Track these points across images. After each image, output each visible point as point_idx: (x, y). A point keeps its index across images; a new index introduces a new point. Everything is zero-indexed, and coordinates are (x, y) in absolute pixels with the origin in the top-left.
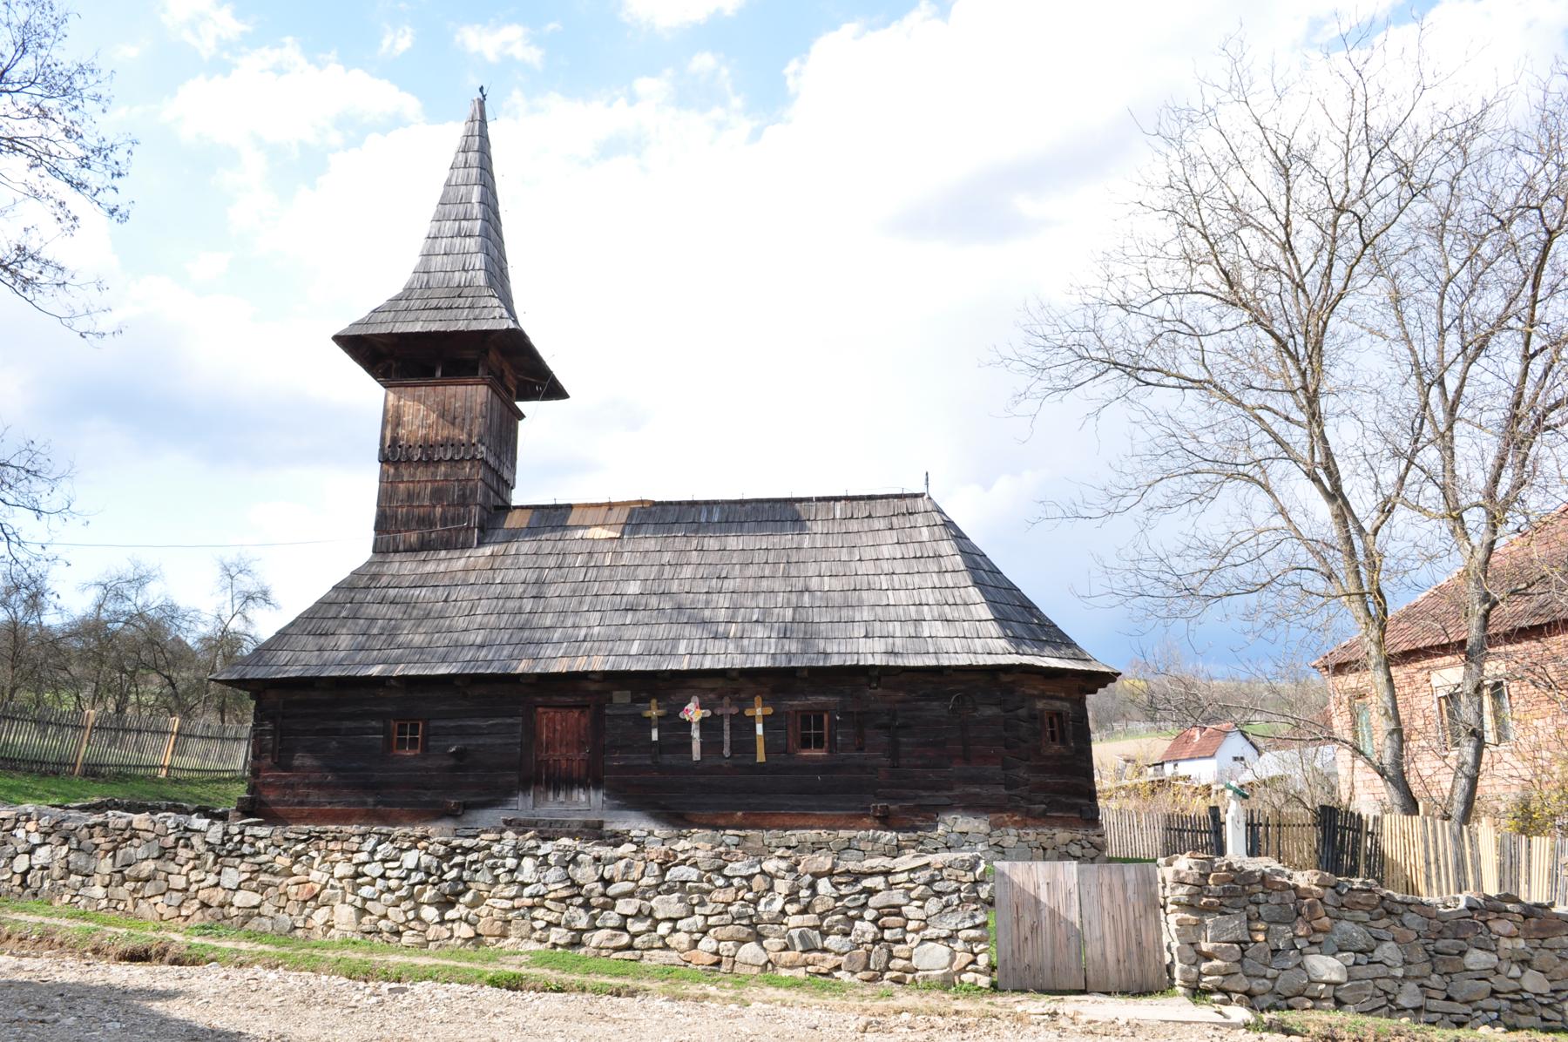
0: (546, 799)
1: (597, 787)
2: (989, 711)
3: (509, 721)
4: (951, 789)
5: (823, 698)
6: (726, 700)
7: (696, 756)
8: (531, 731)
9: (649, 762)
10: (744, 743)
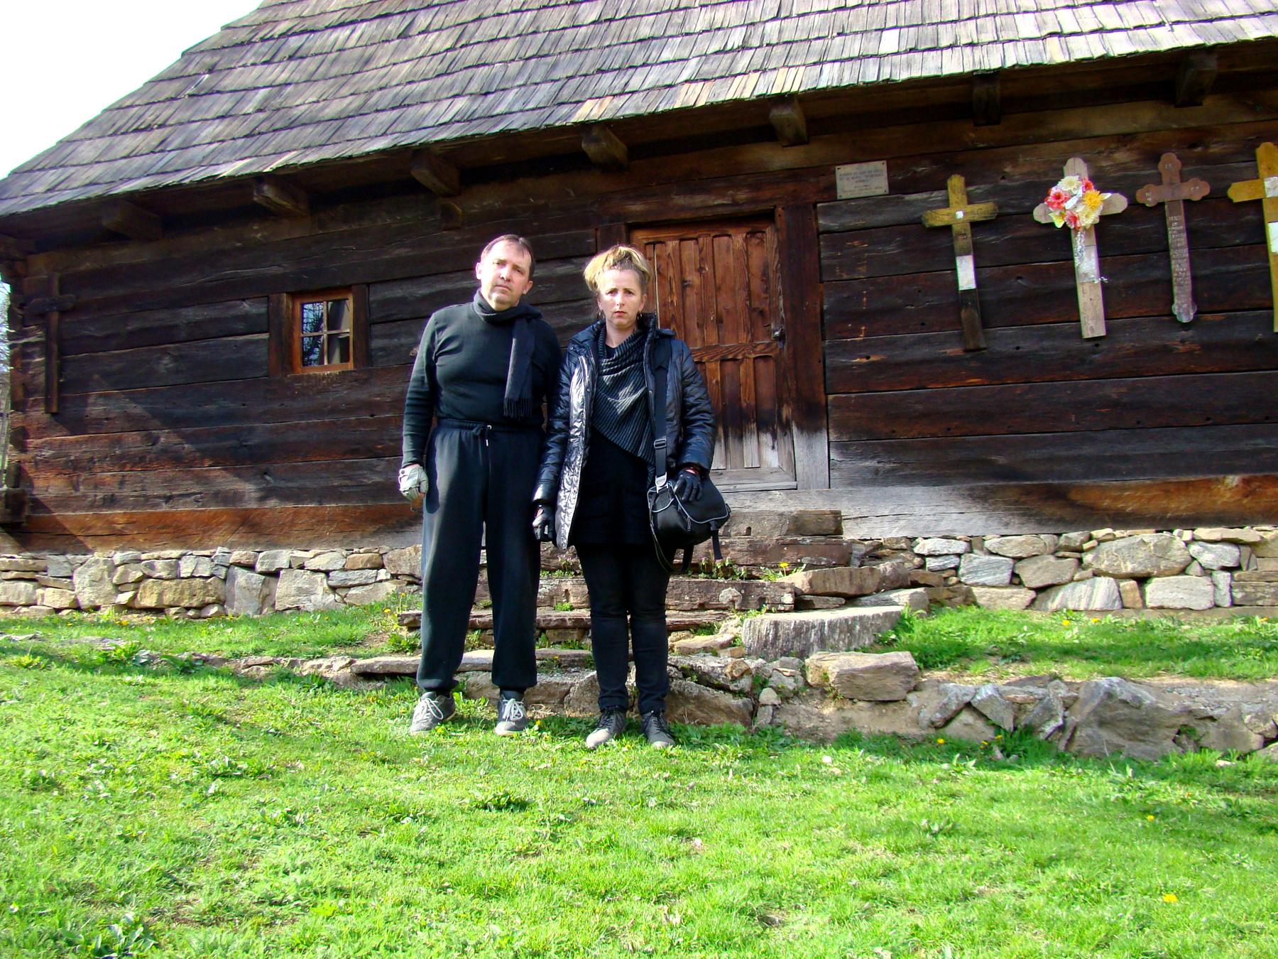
6: (1170, 163)
7: (1092, 321)
9: (953, 351)
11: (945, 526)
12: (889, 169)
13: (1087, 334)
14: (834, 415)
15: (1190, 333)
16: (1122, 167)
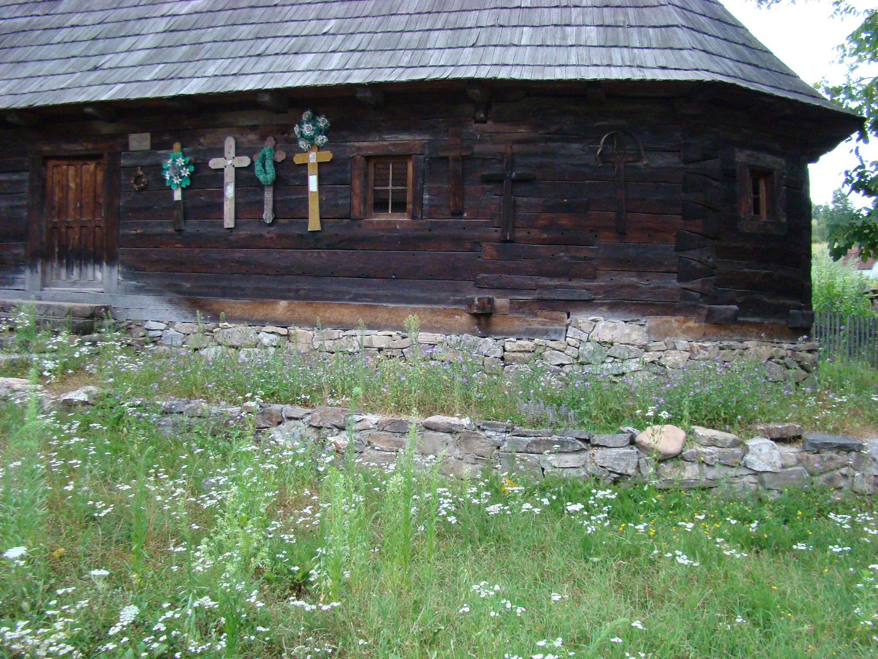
0: (58, 276)
1: (112, 261)
2: (661, 161)
3: (16, 177)
4: (594, 278)
5: (405, 138)
7: (229, 221)
8: (41, 189)
9: (170, 230)
10: (291, 205)
11: (158, 317)
12: (152, 137)
13: (226, 226)
14: (121, 257)
15: (272, 229)
16: (251, 142)
